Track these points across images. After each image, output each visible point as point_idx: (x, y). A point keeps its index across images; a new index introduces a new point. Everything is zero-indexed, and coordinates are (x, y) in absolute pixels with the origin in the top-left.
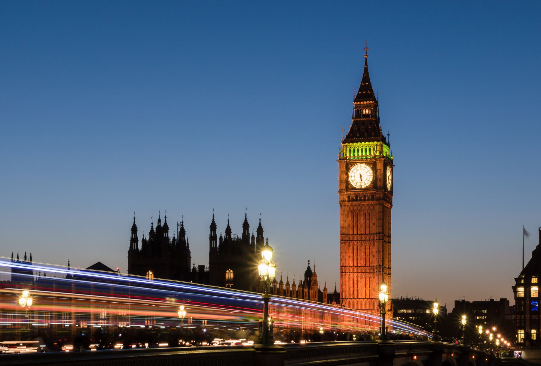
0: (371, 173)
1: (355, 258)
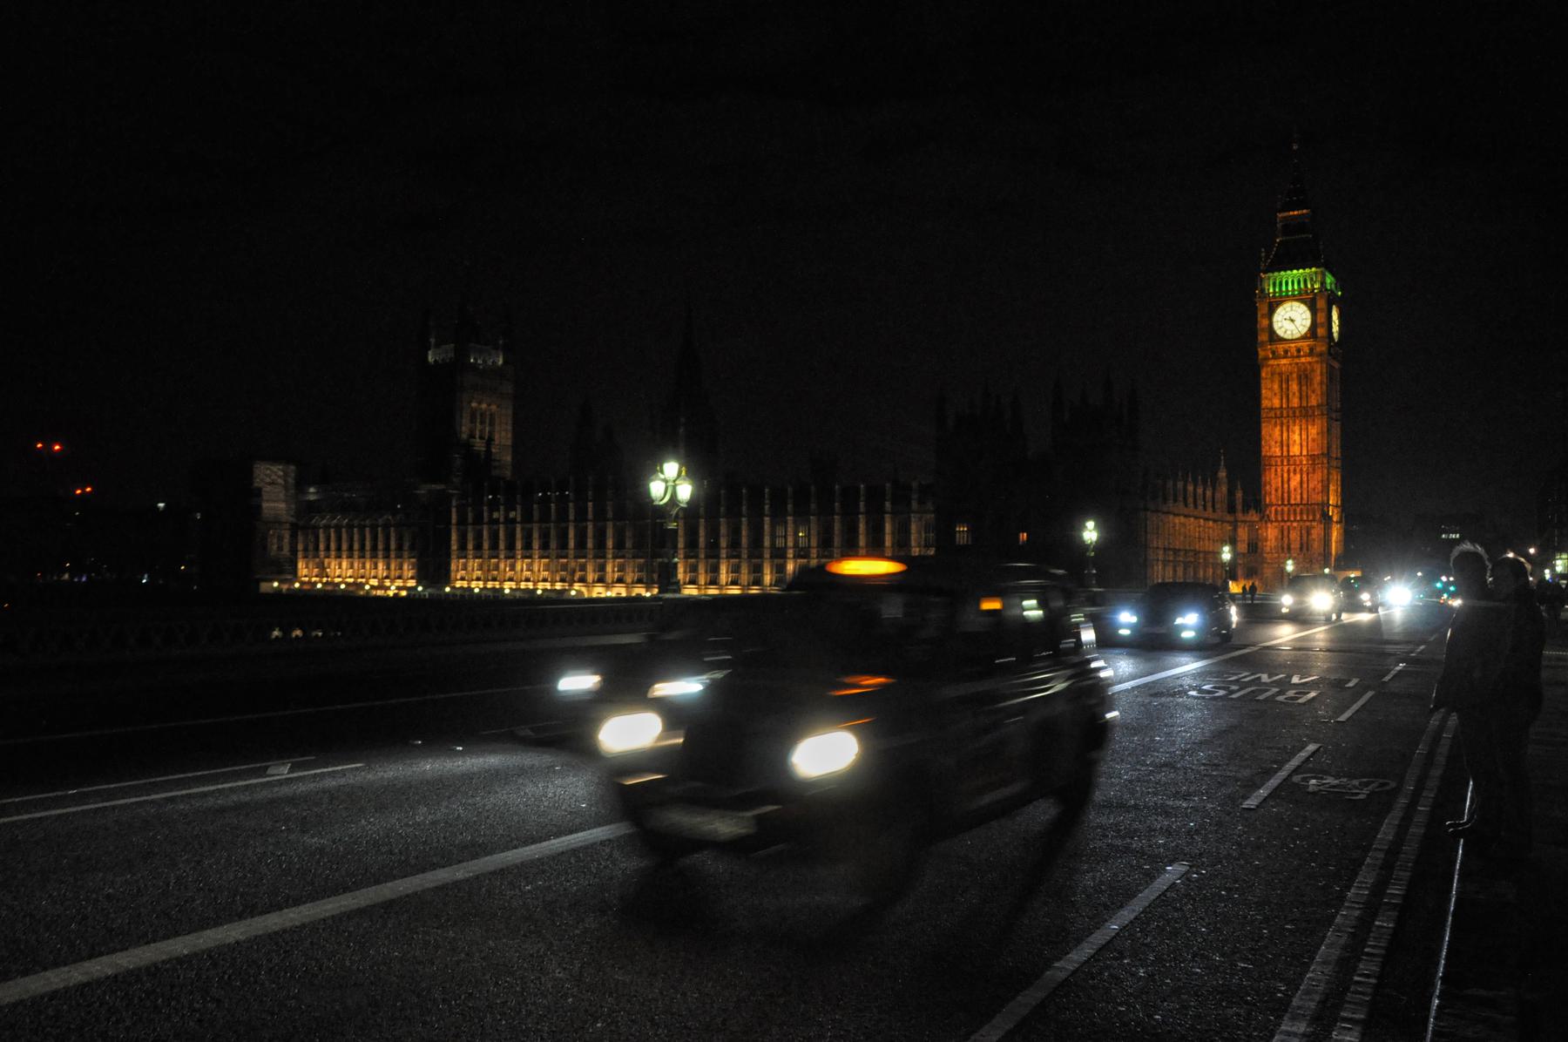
0: (1308, 315)
1: (1285, 443)
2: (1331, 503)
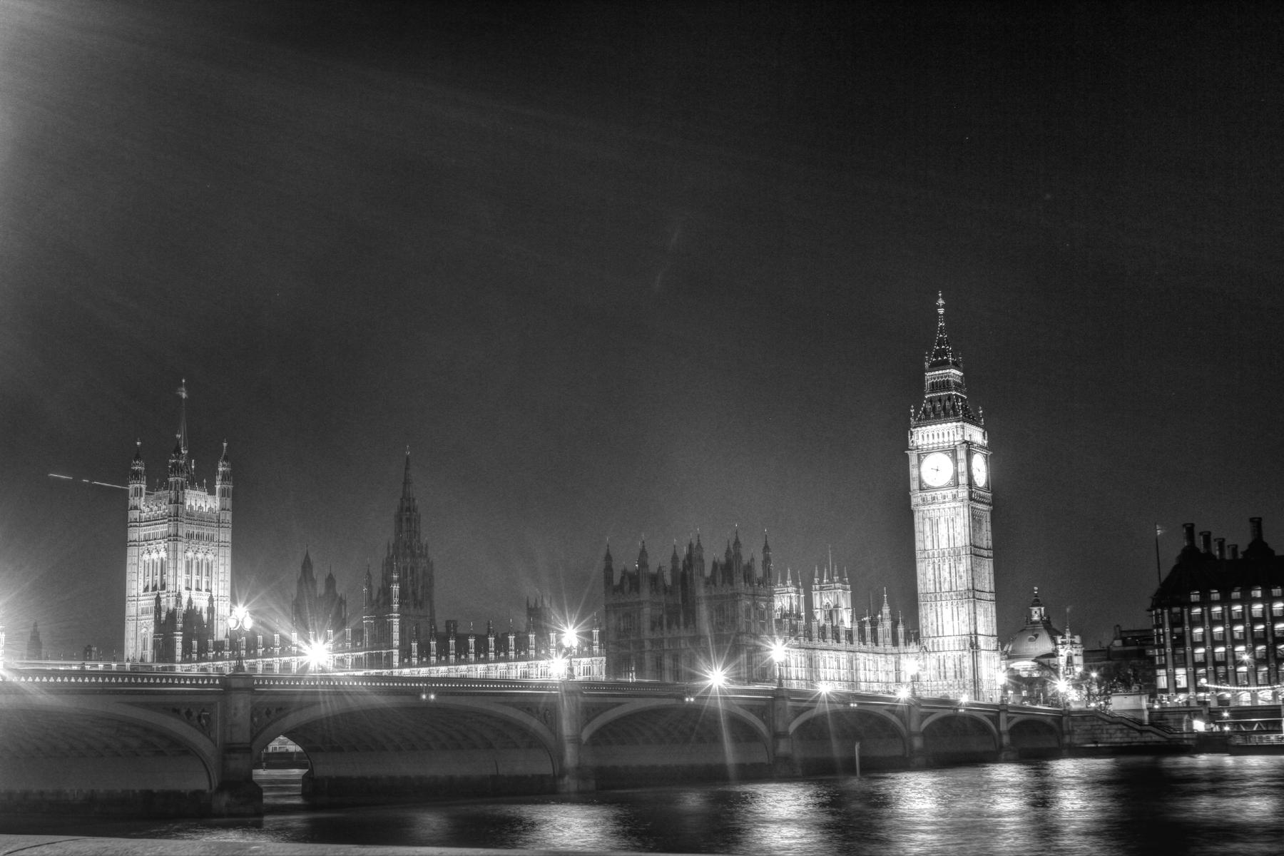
1: (937, 580)
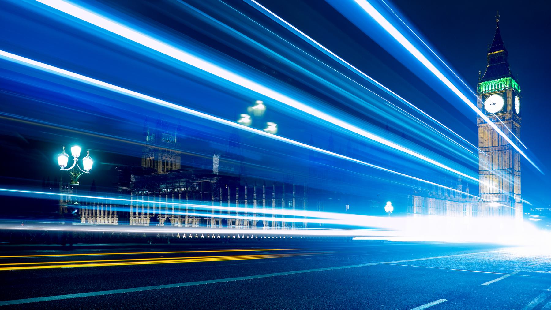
2: (515, 192)
